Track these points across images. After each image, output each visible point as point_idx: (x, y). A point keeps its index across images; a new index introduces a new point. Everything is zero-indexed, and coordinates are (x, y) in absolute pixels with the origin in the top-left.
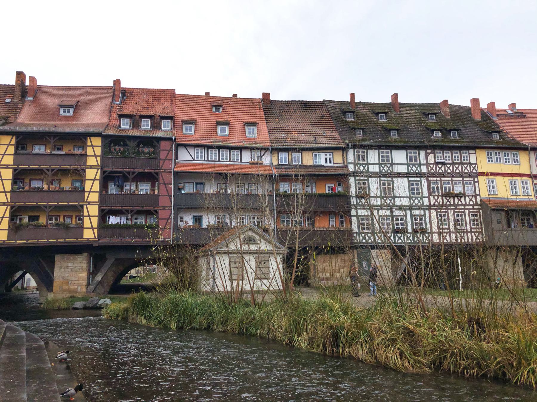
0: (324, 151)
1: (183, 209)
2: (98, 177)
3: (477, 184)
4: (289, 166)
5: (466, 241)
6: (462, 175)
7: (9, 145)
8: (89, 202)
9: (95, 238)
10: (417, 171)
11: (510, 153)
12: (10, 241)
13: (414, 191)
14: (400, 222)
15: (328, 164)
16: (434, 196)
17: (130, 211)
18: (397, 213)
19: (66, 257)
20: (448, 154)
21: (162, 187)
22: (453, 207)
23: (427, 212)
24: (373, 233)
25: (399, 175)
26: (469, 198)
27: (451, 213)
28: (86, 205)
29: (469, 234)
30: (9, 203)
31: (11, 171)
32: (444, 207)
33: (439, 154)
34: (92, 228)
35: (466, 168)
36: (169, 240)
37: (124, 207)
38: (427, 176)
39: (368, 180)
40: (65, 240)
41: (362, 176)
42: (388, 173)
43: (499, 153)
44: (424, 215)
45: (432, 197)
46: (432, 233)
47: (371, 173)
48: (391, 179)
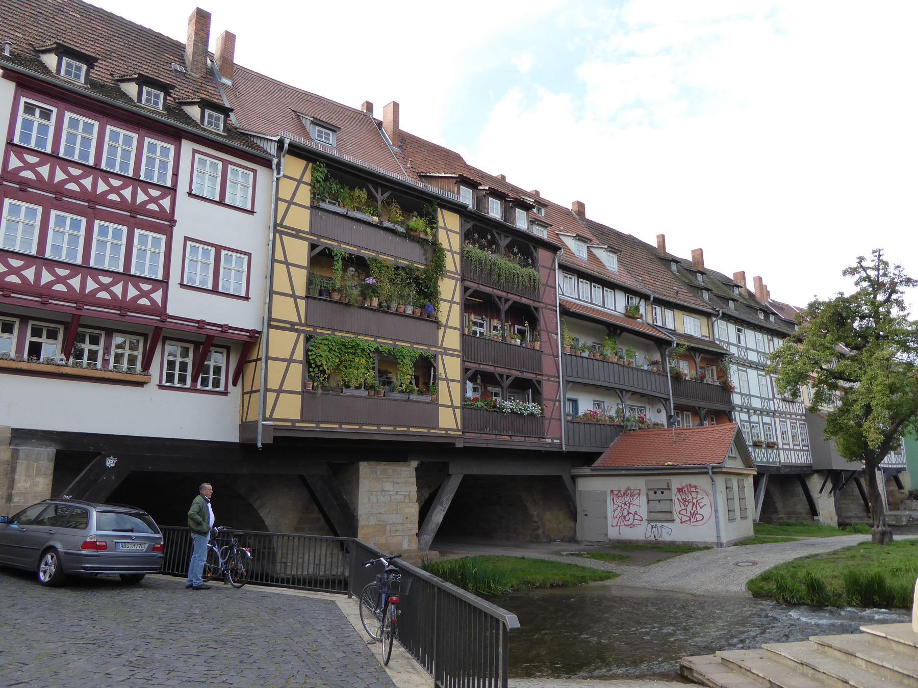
0: (693, 315)
1: (571, 384)
2: (457, 298)
7: (300, 181)
8: (446, 349)
9: (457, 430)
12: (309, 422)
17: (505, 377)
19: (379, 467)
21: (544, 336)
28: (442, 354)
30: (306, 325)
31: (305, 245)
34: (453, 407)
36: (558, 441)
37: (497, 369)
40: (395, 428)
48: (745, 369)
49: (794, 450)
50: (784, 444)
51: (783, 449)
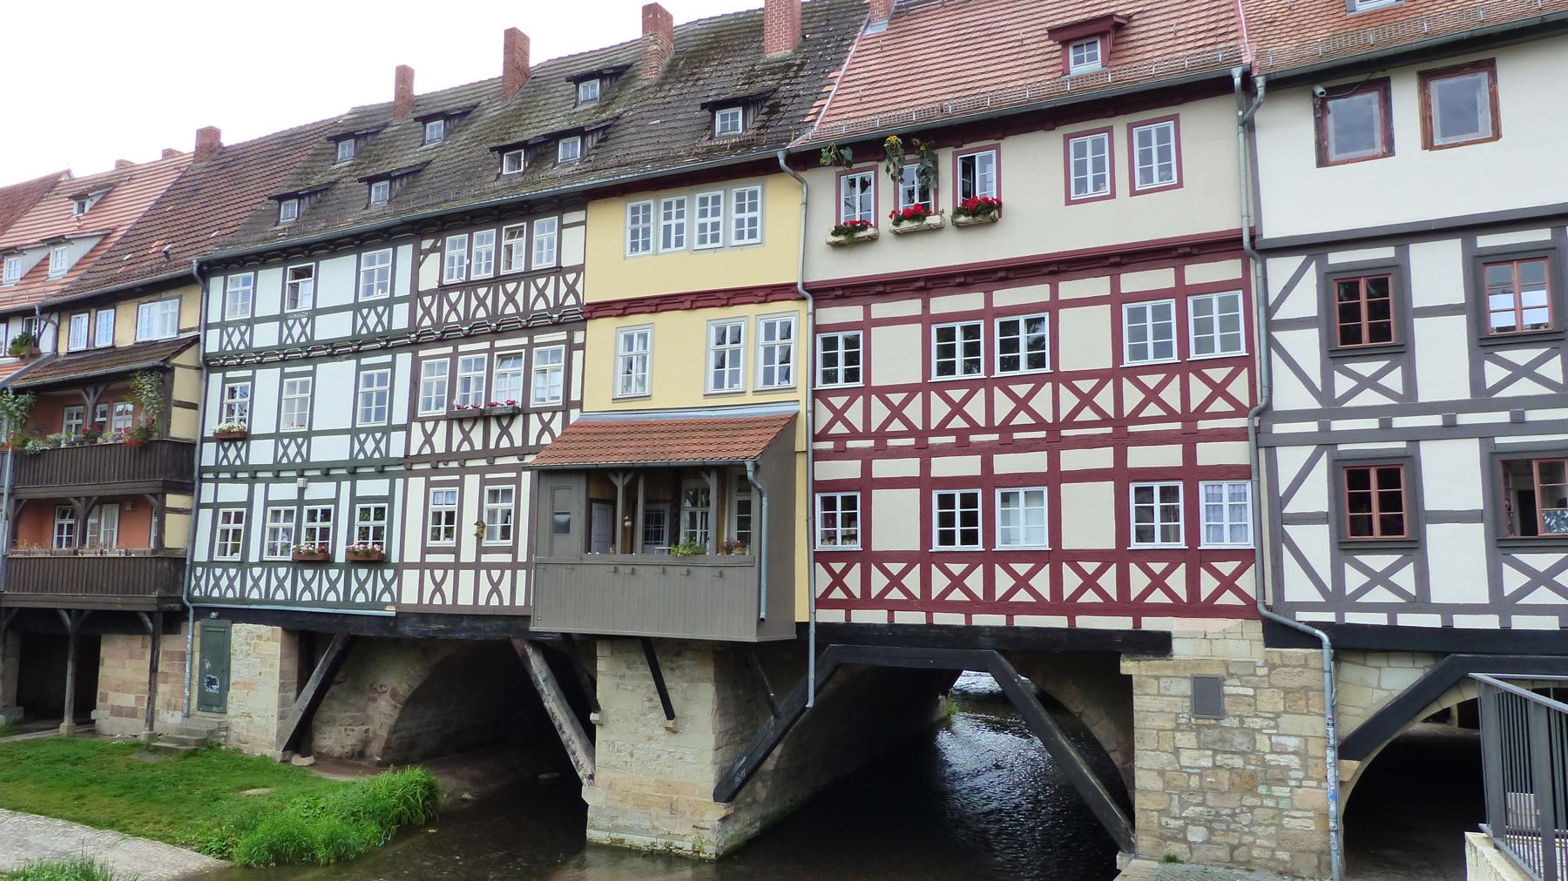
0: (164, 295)
3: (577, 355)
4: (92, 355)
5: (507, 602)
6: (530, 325)
10: (379, 329)
11: (728, 195)
13: (374, 402)
14: (318, 525)
15: (170, 334)
16: (423, 421)
18: (320, 491)
20: (485, 241)
22: (483, 463)
23: (399, 482)
24: (243, 565)
25: (333, 351)
26: (541, 420)
27: (472, 482)
29: (521, 574)
32: (454, 465)
33: (455, 245)
35: (541, 293)
38: (414, 340)
39: (252, 379)
41: (240, 366)
42: (304, 347)
43: (680, 204)
44: (390, 499)
45: (420, 424)
46: (399, 568)
47: (258, 351)
49: (477, 566)
50: (426, 550)
51: (421, 566)
